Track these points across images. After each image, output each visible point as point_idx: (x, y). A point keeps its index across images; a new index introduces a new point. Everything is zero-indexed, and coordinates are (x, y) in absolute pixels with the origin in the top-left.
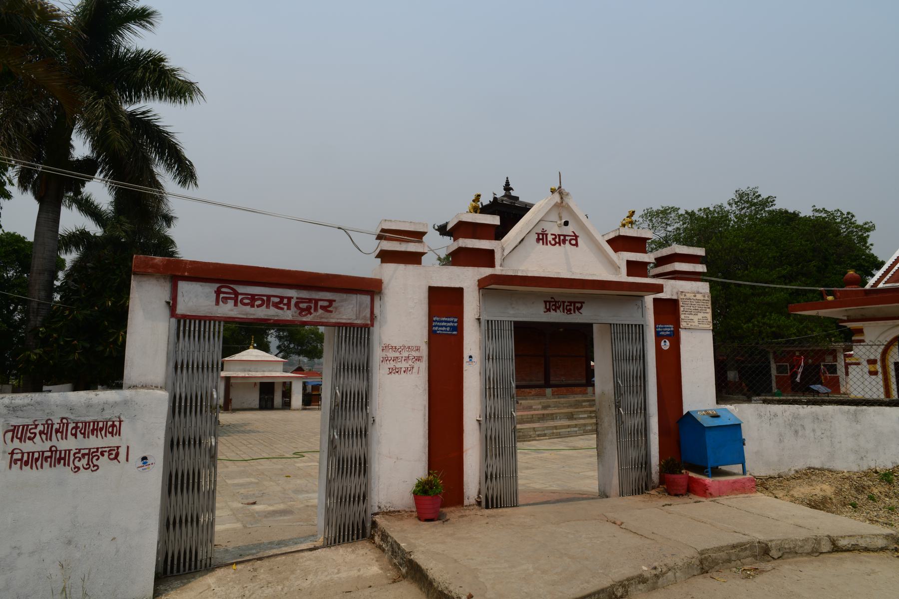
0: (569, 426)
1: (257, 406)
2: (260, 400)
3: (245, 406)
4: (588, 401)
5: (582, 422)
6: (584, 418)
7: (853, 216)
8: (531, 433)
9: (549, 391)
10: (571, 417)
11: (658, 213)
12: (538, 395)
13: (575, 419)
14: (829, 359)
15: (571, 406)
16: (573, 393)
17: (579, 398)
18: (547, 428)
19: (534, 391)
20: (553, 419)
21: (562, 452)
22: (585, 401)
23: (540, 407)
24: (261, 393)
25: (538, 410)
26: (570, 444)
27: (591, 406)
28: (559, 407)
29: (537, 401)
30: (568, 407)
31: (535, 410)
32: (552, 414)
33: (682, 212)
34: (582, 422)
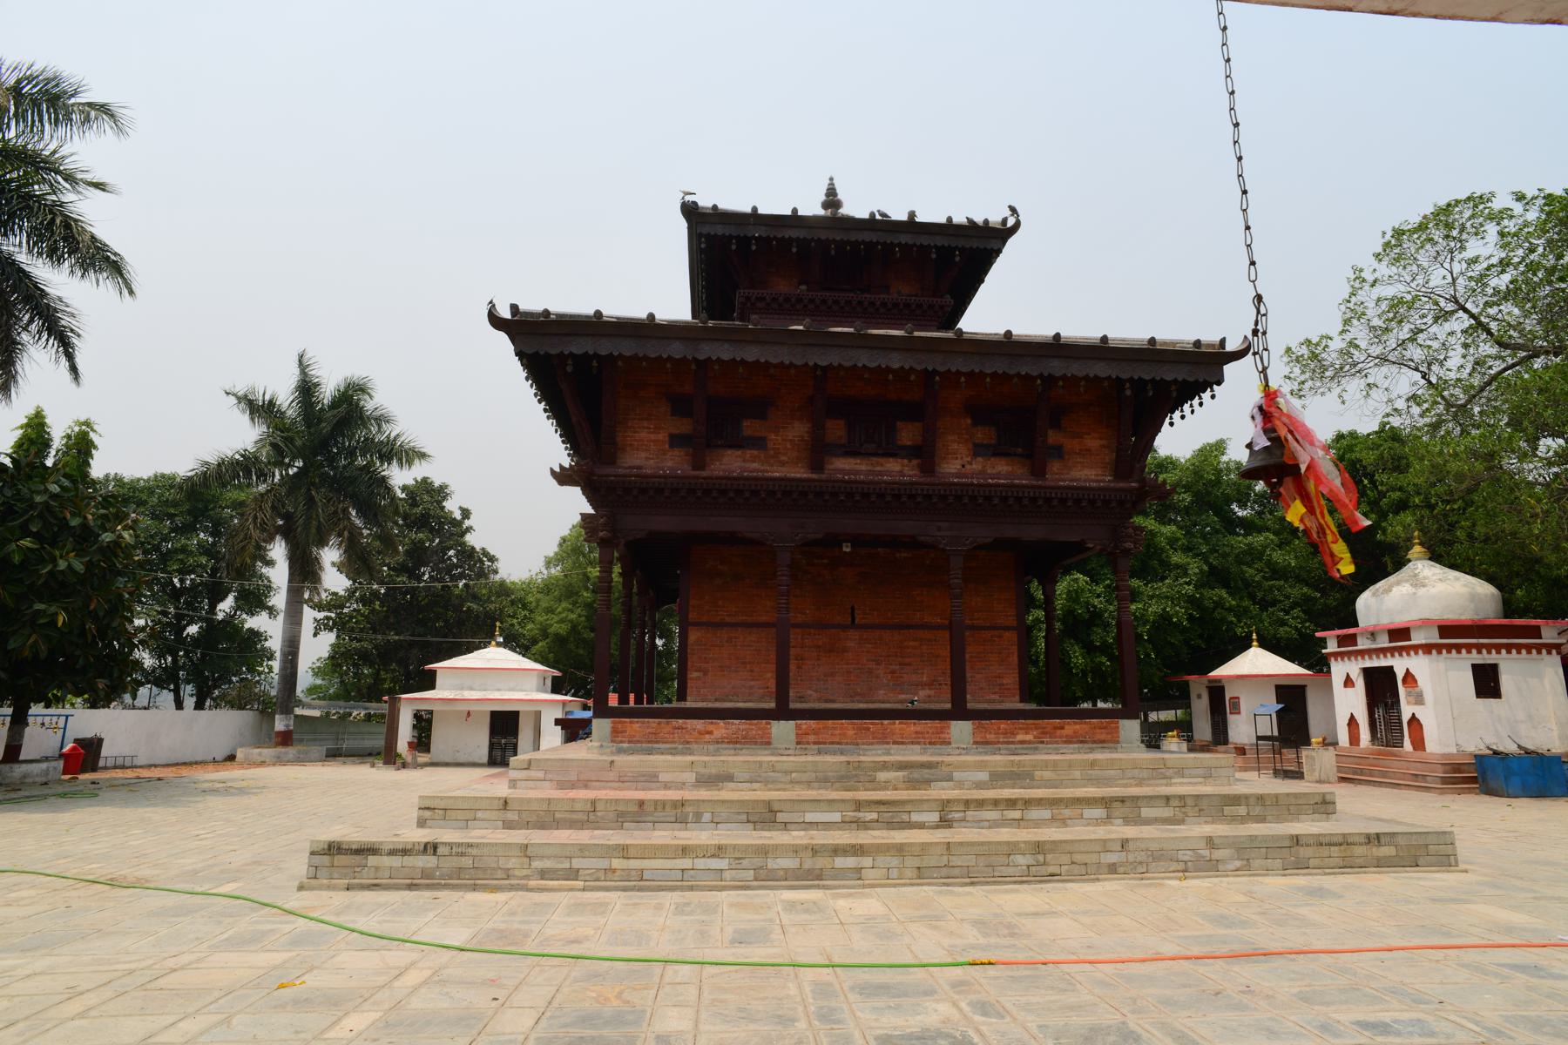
1: (485, 759)
2: (492, 746)
3: (462, 759)
6: (828, 826)
8: (512, 863)
9: (783, 730)
10: (766, 816)
12: (735, 742)
13: (785, 826)
15: (824, 781)
16: (884, 739)
18: (583, 850)
19: (720, 728)
20: (682, 821)
22: (885, 766)
23: (690, 777)
24: (494, 731)
25: (682, 786)
27: (913, 784)
28: (767, 783)
30: (808, 784)
31: (666, 786)
33: (1497, 205)
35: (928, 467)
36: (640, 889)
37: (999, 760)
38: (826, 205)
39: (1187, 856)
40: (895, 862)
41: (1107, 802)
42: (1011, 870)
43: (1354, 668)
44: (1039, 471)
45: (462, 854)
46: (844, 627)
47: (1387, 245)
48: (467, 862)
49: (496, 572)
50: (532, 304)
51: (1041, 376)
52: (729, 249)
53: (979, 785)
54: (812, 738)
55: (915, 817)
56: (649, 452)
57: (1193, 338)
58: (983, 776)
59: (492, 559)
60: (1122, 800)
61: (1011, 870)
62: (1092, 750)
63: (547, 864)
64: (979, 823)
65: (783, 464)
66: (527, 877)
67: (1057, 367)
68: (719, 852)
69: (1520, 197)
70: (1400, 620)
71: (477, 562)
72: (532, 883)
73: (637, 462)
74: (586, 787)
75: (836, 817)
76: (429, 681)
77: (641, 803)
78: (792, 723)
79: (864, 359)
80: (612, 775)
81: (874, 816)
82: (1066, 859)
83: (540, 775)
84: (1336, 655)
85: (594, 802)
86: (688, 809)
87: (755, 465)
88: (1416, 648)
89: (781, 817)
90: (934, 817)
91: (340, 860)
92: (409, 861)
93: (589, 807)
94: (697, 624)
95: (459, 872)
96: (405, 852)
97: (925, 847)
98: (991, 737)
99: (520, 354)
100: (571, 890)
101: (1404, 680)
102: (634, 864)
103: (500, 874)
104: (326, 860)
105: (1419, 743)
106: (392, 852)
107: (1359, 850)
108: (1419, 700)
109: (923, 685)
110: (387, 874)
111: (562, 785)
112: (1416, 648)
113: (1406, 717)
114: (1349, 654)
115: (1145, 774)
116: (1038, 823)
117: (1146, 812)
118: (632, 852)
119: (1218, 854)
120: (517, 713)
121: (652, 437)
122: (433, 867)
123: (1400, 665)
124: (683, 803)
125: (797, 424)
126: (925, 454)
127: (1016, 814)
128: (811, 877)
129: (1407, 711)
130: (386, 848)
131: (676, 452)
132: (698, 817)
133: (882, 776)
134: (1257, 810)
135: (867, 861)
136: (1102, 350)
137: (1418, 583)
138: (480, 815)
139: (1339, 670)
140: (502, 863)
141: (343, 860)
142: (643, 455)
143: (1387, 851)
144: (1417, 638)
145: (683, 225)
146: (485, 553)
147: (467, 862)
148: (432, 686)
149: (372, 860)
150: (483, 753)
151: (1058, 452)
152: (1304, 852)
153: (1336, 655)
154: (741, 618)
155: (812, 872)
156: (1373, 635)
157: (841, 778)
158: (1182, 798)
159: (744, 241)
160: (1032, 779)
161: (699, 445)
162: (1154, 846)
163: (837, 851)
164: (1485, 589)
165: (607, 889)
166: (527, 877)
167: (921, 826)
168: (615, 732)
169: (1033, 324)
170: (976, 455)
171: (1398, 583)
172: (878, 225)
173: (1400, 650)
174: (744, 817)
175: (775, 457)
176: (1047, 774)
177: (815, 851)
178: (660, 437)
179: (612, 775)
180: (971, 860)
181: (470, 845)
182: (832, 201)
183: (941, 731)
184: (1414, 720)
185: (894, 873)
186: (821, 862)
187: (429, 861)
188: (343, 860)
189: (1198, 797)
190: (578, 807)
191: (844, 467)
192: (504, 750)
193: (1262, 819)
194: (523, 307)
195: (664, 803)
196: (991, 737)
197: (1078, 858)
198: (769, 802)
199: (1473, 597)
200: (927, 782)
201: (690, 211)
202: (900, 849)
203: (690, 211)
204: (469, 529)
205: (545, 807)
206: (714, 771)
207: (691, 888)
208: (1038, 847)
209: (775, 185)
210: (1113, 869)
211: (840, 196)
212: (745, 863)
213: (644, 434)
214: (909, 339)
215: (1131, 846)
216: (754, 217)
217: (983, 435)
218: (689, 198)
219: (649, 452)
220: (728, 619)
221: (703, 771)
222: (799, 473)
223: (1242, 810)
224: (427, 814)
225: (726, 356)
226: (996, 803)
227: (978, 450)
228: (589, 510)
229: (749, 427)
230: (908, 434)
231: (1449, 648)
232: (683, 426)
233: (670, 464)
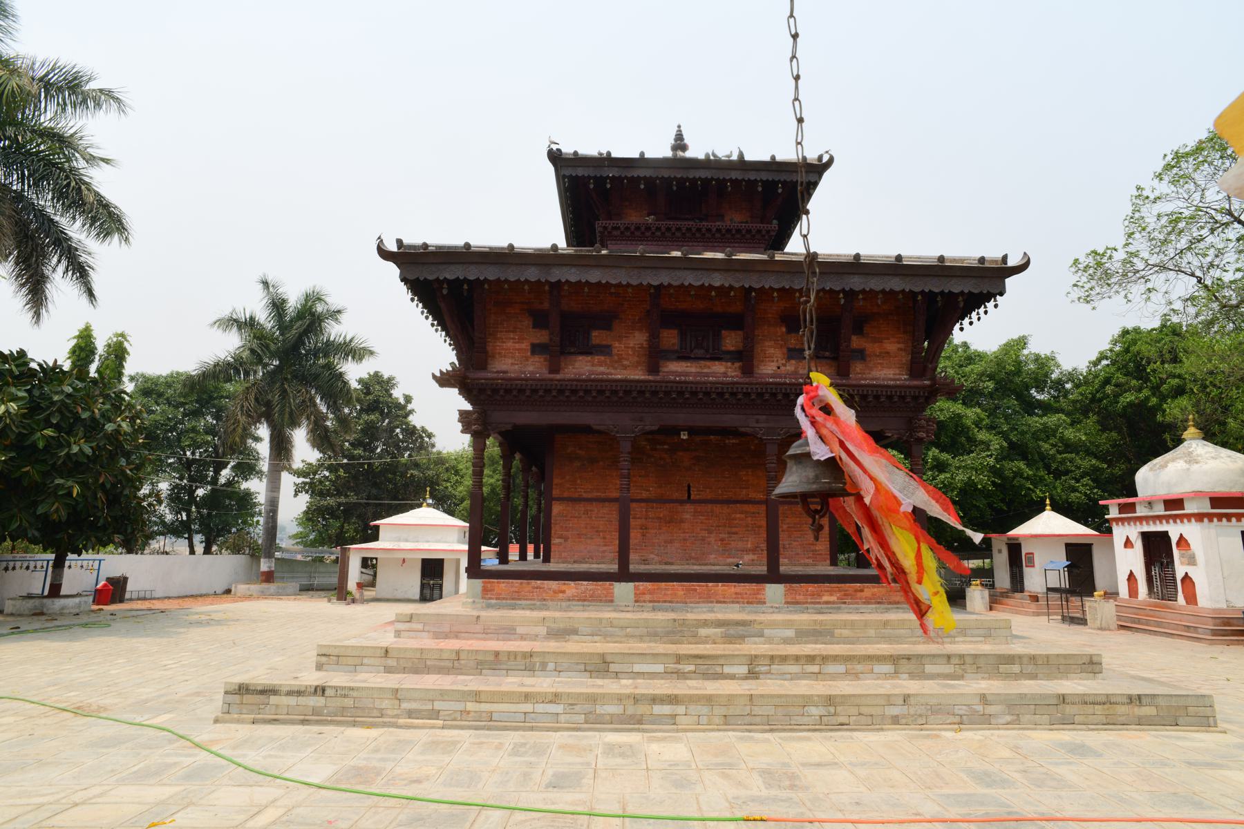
1: (417, 596)
2: (423, 586)
3: (399, 596)
8: (385, 704)
9: (624, 590)
10: (601, 666)
12: (583, 599)
13: (617, 675)
15: (653, 635)
16: (708, 599)
18: (443, 694)
19: (571, 588)
20: (530, 669)
22: (705, 623)
23: (542, 630)
24: (424, 575)
25: (535, 637)
27: (729, 639)
28: (606, 637)
30: (641, 638)
31: (523, 638)
35: (748, 370)
36: (489, 729)
37: (804, 618)
39: (962, 710)
41: (895, 659)
42: (805, 720)
43: (1133, 532)
45: (345, 696)
46: (681, 502)
47: (1168, 167)
48: (348, 702)
49: (433, 446)
50: (414, 238)
51: (843, 290)
52: (591, 189)
53: (786, 641)
54: (648, 597)
55: (727, 670)
56: (515, 358)
57: (978, 255)
58: (790, 633)
59: (430, 436)
60: (909, 658)
61: (805, 720)
62: (887, 610)
63: (414, 706)
64: (782, 676)
65: (625, 368)
67: (856, 283)
68: (555, 698)
70: (1175, 492)
72: (401, 721)
73: (504, 367)
74: (457, 637)
75: (659, 668)
77: (497, 654)
78: (631, 584)
79: (691, 279)
80: (478, 628)
81: (692, 668)
82: (854, 710)
83: (420, 627)
84: (1117, 520)
85: (458, 652)
86: (536, 659)
87: (602, 369)
88: (1189, 517)
89: (613, 667)
90: (743, 670)
91: (248, 698)
93: (454, 656)
94: (559, 499)
96: (299, 693)
97: (731, 698)
98: (800, 598)
99: (404, 279)
100: (433, 727)
101: (1178, 544)
103: (376, 713)
104: (237, 698)
105: (1191, 598)
106: (290, 693)
107: (1122, 709)
108: (1192, 561)
109: (747, 551)
110: (285, 711)
111: (437, 636)
112: (1189, 517)
113: (1179, 575)
114: (1129, 520)
116: (834, 677)
117: (929, 668)
118: (483, 698)
119: (991, 710)
120: (442, 561)
121: (517, 346)
122: (321, 706)
123: (1174, 531)
125: (637, 334)
126: (746, 358)
127: (815, 669)
128: (633, 722)
129: (1180, 570)
130: (285, 689)
131: (537, 358)
132: (544, 667)
133: (703, 632)
134: (1030, 669)
135: (681, 709)
136: (897, 268)
137: (1191, 459)
138: (365, 661)
139: (1120, 533)
140: (378, 704)
141: (250, 699)
142: (510, 361)
144: (1190, 508)
145: (550, 169)
146: (424, 430)
147: (348, 702)
149: (273, 699)
150: (415, 592)
151: (861, 355)
152: (1069, 709)
154: (595, 494)
155: (634, 716)
156: (1150, 504)
157: (668, 634)
158: (961, 656)
159: (600, 181)
160: (832, 635)
162: (933, 701)
163: (655, 700)
165: (462, 728)
166: (397, 716)
167: (732, 677)
168: (485, 590)
170: (789, 358)
171: (1173, 460)
172: (710, 164)
173: (1175, 518)
174: (582, 667)
175: (619, 361)
176: (846, 632)
177: (636, 699)
178: (523, 346)
179: (478, 628)
180: (770, 710)
181: (352, 689)
185: (704, 720)
186: (642, 709)
187: (318, 701)
188: (250, 699)
189: (976, 656)
190: (445, 656)
191: (676, 369)
192: (432, 589)
193: (1034, 677)
194: (406, 241)
195: (515, 654)
196: (800, 598)
197: (864, 710)
198: (603, 655)
200: (742, 638)
201: (556, 157)
202: (709, 700)
203: (556, 157)
204: (411, 412)
205: (418, 656)
206: (562, 626)
207: (532, 729)
208: (830, 700)
209: (633, 133)
210: (896, 720)
211: (686, 141)
212: (577, 708)
213: (510, 344)
214: (728, 262)
215: (912, 701)
216: (607, 161)
218: (554, 147)
219: (515, 358)
220: (585, 495)
221: (553, 625)
222: (638, 375)
223: (1016, 668)
224: (324, 659)
225: (573, 279)
226: (797, 658)
228: (468, 407)
229: (597, 337)
230: (731, 341)
231: (1220, 517)
232: (542, 337)
233: (531, 368)
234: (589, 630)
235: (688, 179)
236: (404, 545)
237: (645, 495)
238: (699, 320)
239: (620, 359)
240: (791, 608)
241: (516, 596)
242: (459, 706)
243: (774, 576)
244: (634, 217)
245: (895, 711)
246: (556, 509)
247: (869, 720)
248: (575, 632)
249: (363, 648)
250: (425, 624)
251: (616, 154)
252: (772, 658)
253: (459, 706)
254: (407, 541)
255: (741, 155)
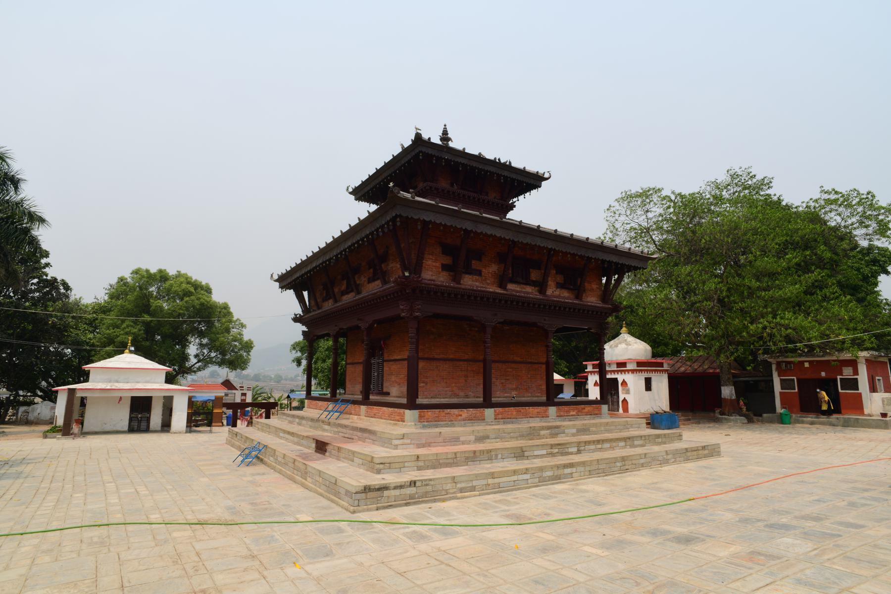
0: (515, 472)
1: (126, 428)
2: (131, 419)
3: (108, 428)
4: (549, 428)
5: (538, 463)
6: (542, 456)
7: (873, 196)
8: (449, 486)
9: (489, 412)
10: (520, 454)
11: (639, 195)
14: (847, 372)
16: (527, 416)
17: (536, 423)
18: (477, 477)
19: (465, 413)
20: (490, 459)
21: (492, 534)
22: (543, 428)
23: (472, 438)
25: (469, 443)
26: (514, 509)
27: (553, 435)
29: (469, 429)
31: (463, 443)
32: (489, 451)
33: (664, 193)
34: (538, 463)
35: (542, 291)
38: (441, 139)
40: (582, 469)
41: (625, 439)
44: (578, 297)
45: (427, 485)
48: (429, 488)
53: (573, 435)
54: (500, 416)
55: (571, 450)
58: (574, 431)
59: (67, 287)
60: (629, 438)
63: (463, 485)
65: (488, 284)
66: (454, 493)
69: (673, 192)
70: (621, 359)
71: (54, 290)
75: (544, 452)
76: (85, 376)
77: (475, 452)
80: (441, 439)
81: (557, 450)
83: (409, 441)
84: (591, 372)
85: (455, 454)
86: (493, 453)
88: (628, 371)
89: (526, 454)
90: (575, 450)
92: (403, 491)
94: (422, 359)
95: (426, 494)
96: (401, 487)
98: (562, 413)
100: (475, 496)
101: (622, 384)
102: (496, 481)
103: (444, 493)
105: (626, 410)
106: (395, 488)
107: (701, 452)
108: (628, 392)
109: (513, 389)
111: (419, 446)
112: (628, 371)
113: (621, 399)
115: (619, 427)
116: (606, 450)
117: (636, 443)
118: (496, 475)
119: (669, 457)
120: (151, 397)
123: (620, 378)
124: (490, 451)
126: (542, 287)
127: (599, 446)
128: (557, 479)
129: (622, 396)
130: (392, 486)
131: (445, 273)
132: (496, 455)
133: (543, 432)
134: (664, 440)
135: (574, 470)
137: (628, 344)
138: (406, 464)
140: (445, 487)
142: (430, 273)
143: (706, 452)
144: (630, 367)
147: (429, 488)
148: (86, 380)
149: (386, 493)
152: (689, 454)
153: (591, 372)
154: (442, 356)
155: (543, 478)
157: (528, 435)
159: (439, 159)
160: (589, 430)
161: (454, 269)
163: (566, 466)
164: (648, 348)
165: (488, 494)
166: (454, 493)
167: (571, 453)
168: (421, 417)
169: (548, 224)
173: (621, 371)
175: (482, 281)
176: (594, 429)
177: (558, 467)
178: (437, 264)
179: (441, 439)
181: (430, 480)
182: (445, 137)
183: (546, 411)
184: (625, 400)
186: (560, 472)
187: (412, 490)
190: (449, 456)
192: (140, 422)
196: (562, 413)
197: (634, 462)
198: (521, 448)
199: (646, 350)
202: (583, 464)
206: (482, 434)
207: (519, 489)
208: (623, 459)
210: (642, 465)
212: (536, 475)
213: (430, 262)
217: (560, 279)
220: (436, 356)
222: (493, 289)
223: (660, 440)
224: (381, 466)
225: (489, 233)
227: (560, 286)
229: (475, 264)
230: (535, 275)
232: (447, 260)
233: (442, 279)
234: (494, 436)
235: (484, 170)
236: (149, 386)
237: (466, 357)
238: (463, 252)
239: (486, 279)
240: (560, 419)
241: (438, 419)
242: (484, 482)
243: (488, 403)
244: (444, 184)
245: (642, 461)
246: (421, 364)
247: (634, 466)
248: (488, 437)
249: (404, 456)
250: (411, 440)
251: (528, 169)
252: (585, 442)
253: (484, 482)
254: (117, 382)
255: (429, 139)
